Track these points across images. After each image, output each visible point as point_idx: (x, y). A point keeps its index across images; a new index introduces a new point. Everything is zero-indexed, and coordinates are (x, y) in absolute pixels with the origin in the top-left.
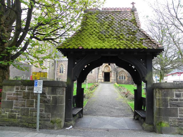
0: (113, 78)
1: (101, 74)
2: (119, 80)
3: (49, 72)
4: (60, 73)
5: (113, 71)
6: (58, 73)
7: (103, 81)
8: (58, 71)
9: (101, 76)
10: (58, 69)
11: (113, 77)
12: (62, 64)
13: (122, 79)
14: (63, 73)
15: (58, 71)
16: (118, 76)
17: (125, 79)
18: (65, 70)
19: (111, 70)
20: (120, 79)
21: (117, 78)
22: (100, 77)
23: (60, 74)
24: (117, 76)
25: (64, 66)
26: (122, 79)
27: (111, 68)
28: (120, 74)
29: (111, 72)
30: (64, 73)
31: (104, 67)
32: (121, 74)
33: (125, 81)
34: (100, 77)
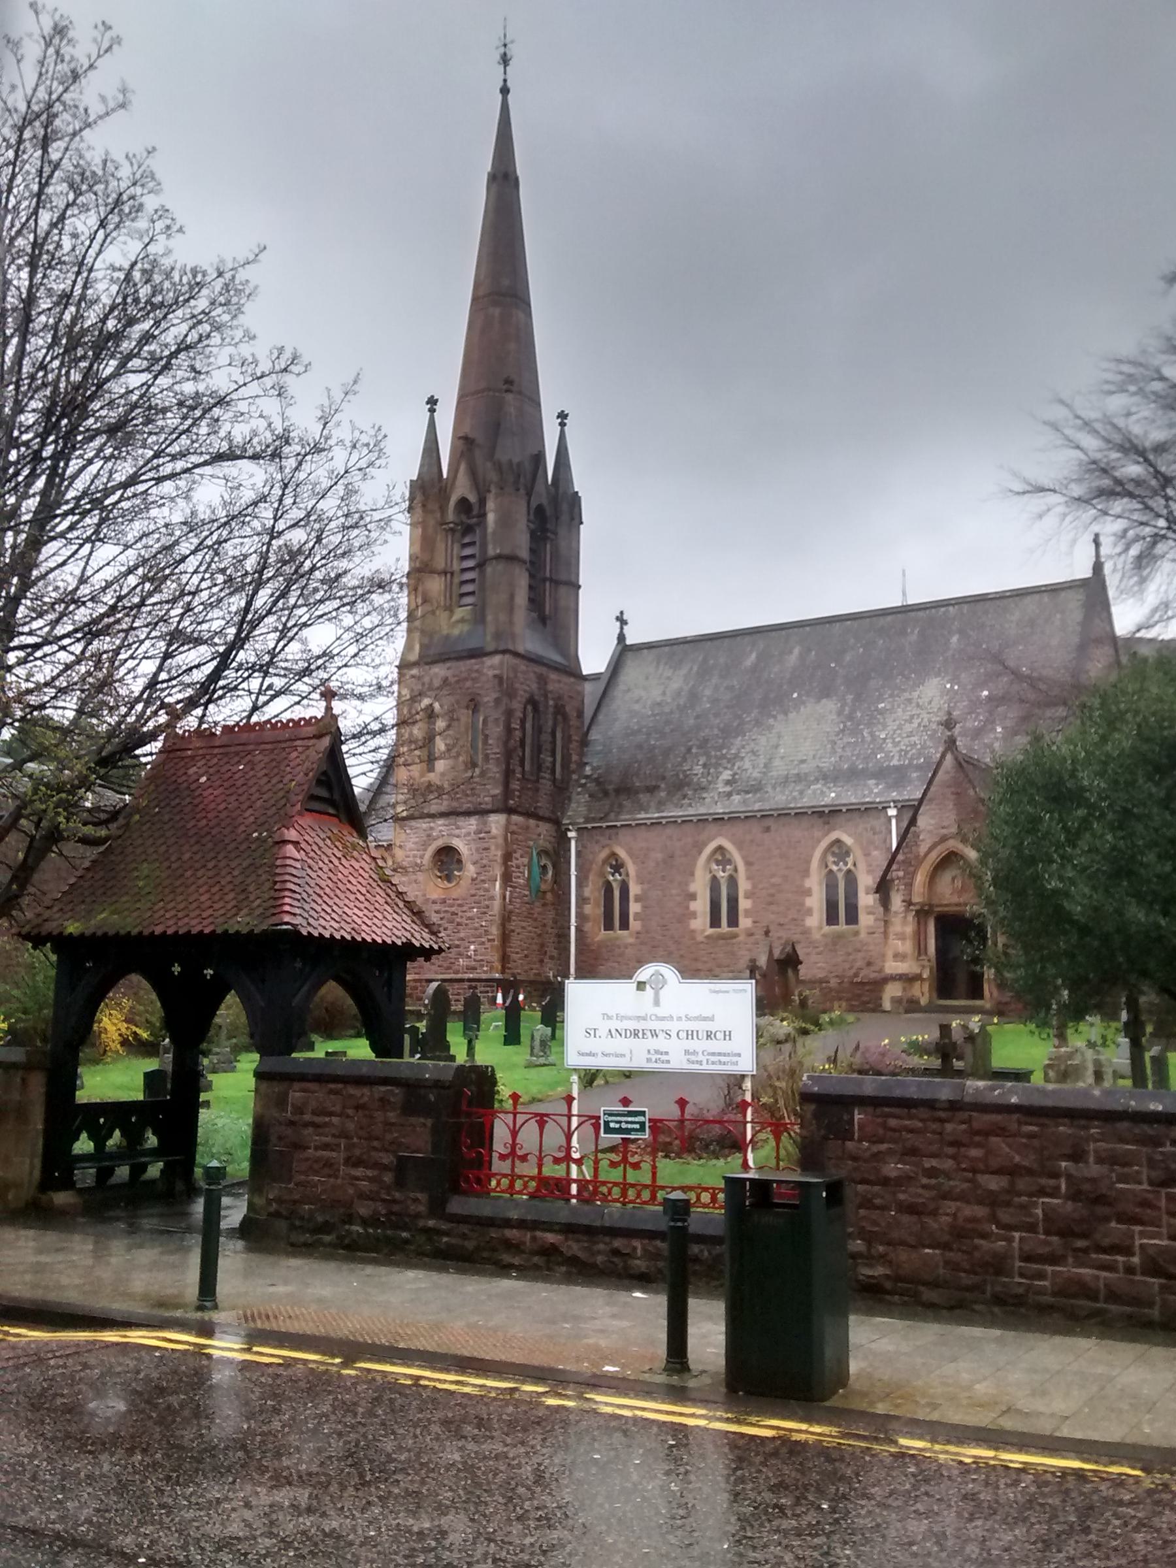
6: (588, 927)
7: (923, 993)
8: (588, 909)
9: (907, 947)
10: (587, 892)
12: (622, 853)
14: (625, 925)
15: (588, 909)
18: (638, 899)
22: (898, 956)
25: (631, 868)
30: (634, 924)
34: (898, 956)
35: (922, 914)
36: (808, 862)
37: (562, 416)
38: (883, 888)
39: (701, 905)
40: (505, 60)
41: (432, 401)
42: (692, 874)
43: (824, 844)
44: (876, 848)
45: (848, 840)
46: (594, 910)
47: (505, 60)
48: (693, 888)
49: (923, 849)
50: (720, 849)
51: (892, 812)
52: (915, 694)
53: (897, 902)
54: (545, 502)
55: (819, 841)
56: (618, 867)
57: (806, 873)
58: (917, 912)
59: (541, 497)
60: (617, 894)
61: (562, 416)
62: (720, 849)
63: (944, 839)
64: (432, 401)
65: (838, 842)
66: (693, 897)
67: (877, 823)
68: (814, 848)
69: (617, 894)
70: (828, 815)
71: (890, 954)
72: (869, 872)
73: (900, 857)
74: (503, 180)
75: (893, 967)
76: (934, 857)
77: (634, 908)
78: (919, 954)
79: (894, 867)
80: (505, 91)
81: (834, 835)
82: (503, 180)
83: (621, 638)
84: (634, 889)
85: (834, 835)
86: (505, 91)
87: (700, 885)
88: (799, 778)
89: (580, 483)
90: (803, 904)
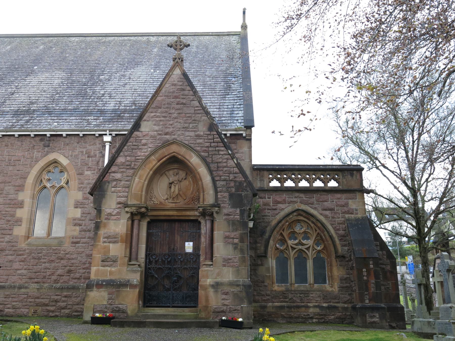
0: (228, 275)
1: (112, 239)
2: (277, 287)
5: (227, 209)
7: (130, 301)
9: (117, 250)
11: (227, 262)
13: (301, 277)
16: (265, 256)
17: (320, 278)
19: (209, 198)
20: (283, 278)
21: (262, 270)
22: (108, 260)
24: (257, 260)
26: (301, 277)
27: (207, 179)
28: (283, 241)
29: (208, 213)
31: (145, 173)
32: (293, 235)
33: (326, 296)
35: (136, 216)
36: (25, 178)
43: (42, 163)
44: (89, 168)
45: (64, 161)
49: (142, 154)
51: (107, 138)
52: (128, 73)
53: (111, 204)
55: (37, 161)
57: (21, 188)
58: (132, 214)
63: (167, 144)
65: (55, 162)
67: (93, 148)
68: (32, 167)
70: (50, 140)
71: (97, 256)
72: (80, 189)
73: (121, 160)
75: (97, 272)
76: (154, 163)
78: (130, 260)
79: (113, 169)
81: (52, 156)
85: (52, 156)
88: (28, 112)
90: (13, 216)
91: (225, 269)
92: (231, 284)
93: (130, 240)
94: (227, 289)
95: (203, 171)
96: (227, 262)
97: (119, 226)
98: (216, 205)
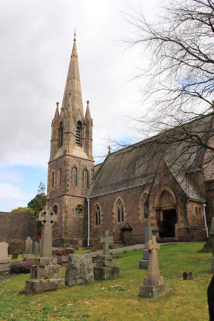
3: (65, 225)
4: (97, 224)
5: (180, 204)
6: (91, 225)
11: (182, 222)
23: (95, 226)
25: (100, 208)
30: (102, 223)
35: (158, 210)
37: (88, 102)
38: (147, 204)
39: (115, 216)
40: (75, 35)
41: (58, 103)
42: (113, 207)
46: (94, 220)
47: (75, 35)
48: (113, 211)
50: (119, 199)
53: (150, 208)
54: (81, 120)
56: (98, 208)
59: (79, 118)
60: (98, 215)
61: (88, 102)
62: (119, 199)
64: (58, 103)
66: (113, 214)
69: (98, 215)
74: (74, 56)
77: (101, 218)
80: (75, 40)
82: (74, 56)
83: (109, 152)
84: (101, 213)
86: (75, 40)
87: (115, 211)
89: (93, 115)
91: (181, 224)
92: (183, 229)
93: (158, 218)
94: (182, 230)
95: (173, 194)
96: (182, 222)
97: (153, 214)
98: (177, 204)
